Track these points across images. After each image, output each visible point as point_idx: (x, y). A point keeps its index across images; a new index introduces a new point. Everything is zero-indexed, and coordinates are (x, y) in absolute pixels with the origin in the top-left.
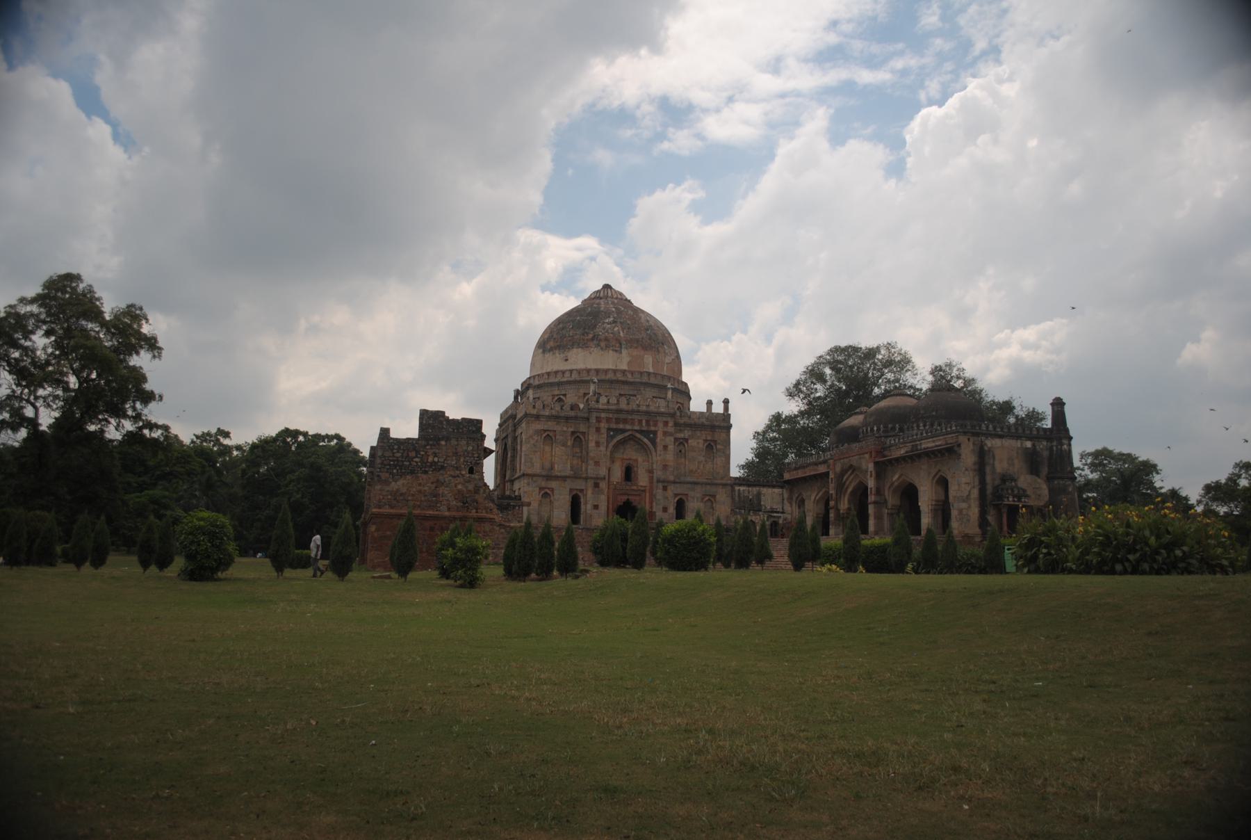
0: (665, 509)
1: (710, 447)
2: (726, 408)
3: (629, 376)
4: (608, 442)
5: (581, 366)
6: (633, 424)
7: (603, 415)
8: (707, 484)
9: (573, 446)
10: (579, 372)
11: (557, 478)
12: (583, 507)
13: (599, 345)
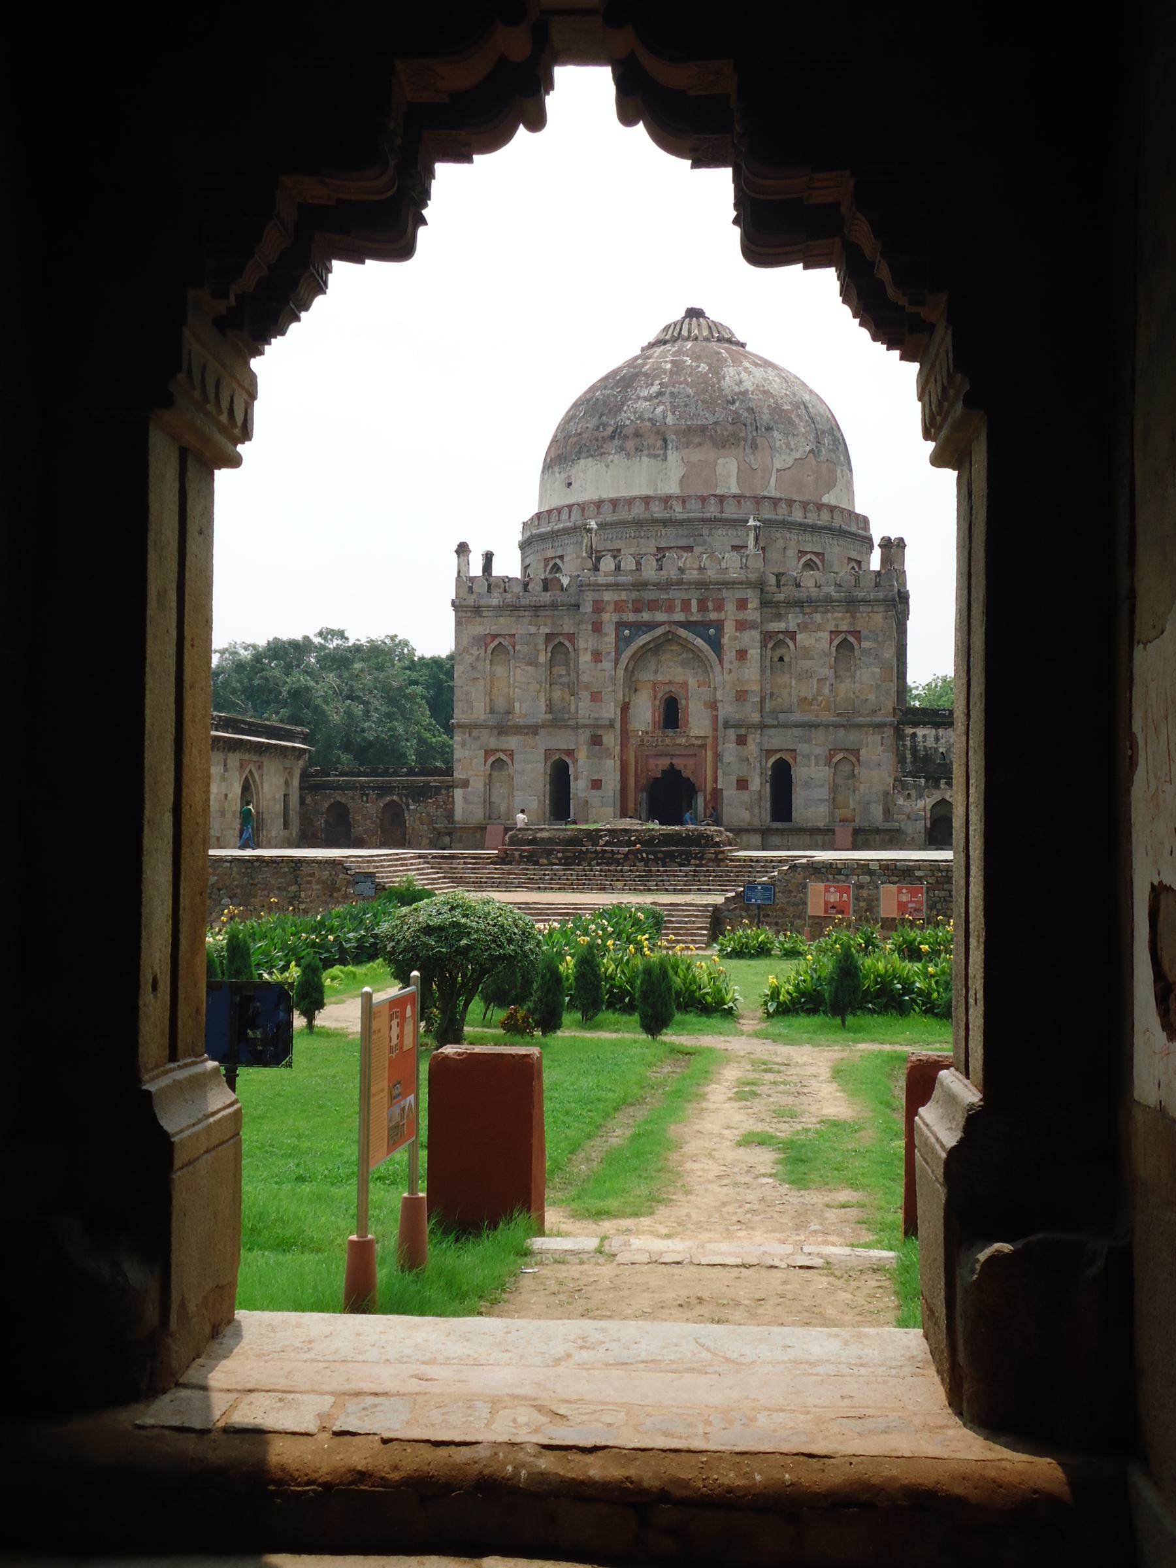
0: (742, 784)
1: (845, 647)
3: (678, 508)
4: (618, 653)
6: (670, 609)
7: (607, 596)
8: (836, 726)
9: (552, 663)
11: (519, 730)
13: (622, 448)
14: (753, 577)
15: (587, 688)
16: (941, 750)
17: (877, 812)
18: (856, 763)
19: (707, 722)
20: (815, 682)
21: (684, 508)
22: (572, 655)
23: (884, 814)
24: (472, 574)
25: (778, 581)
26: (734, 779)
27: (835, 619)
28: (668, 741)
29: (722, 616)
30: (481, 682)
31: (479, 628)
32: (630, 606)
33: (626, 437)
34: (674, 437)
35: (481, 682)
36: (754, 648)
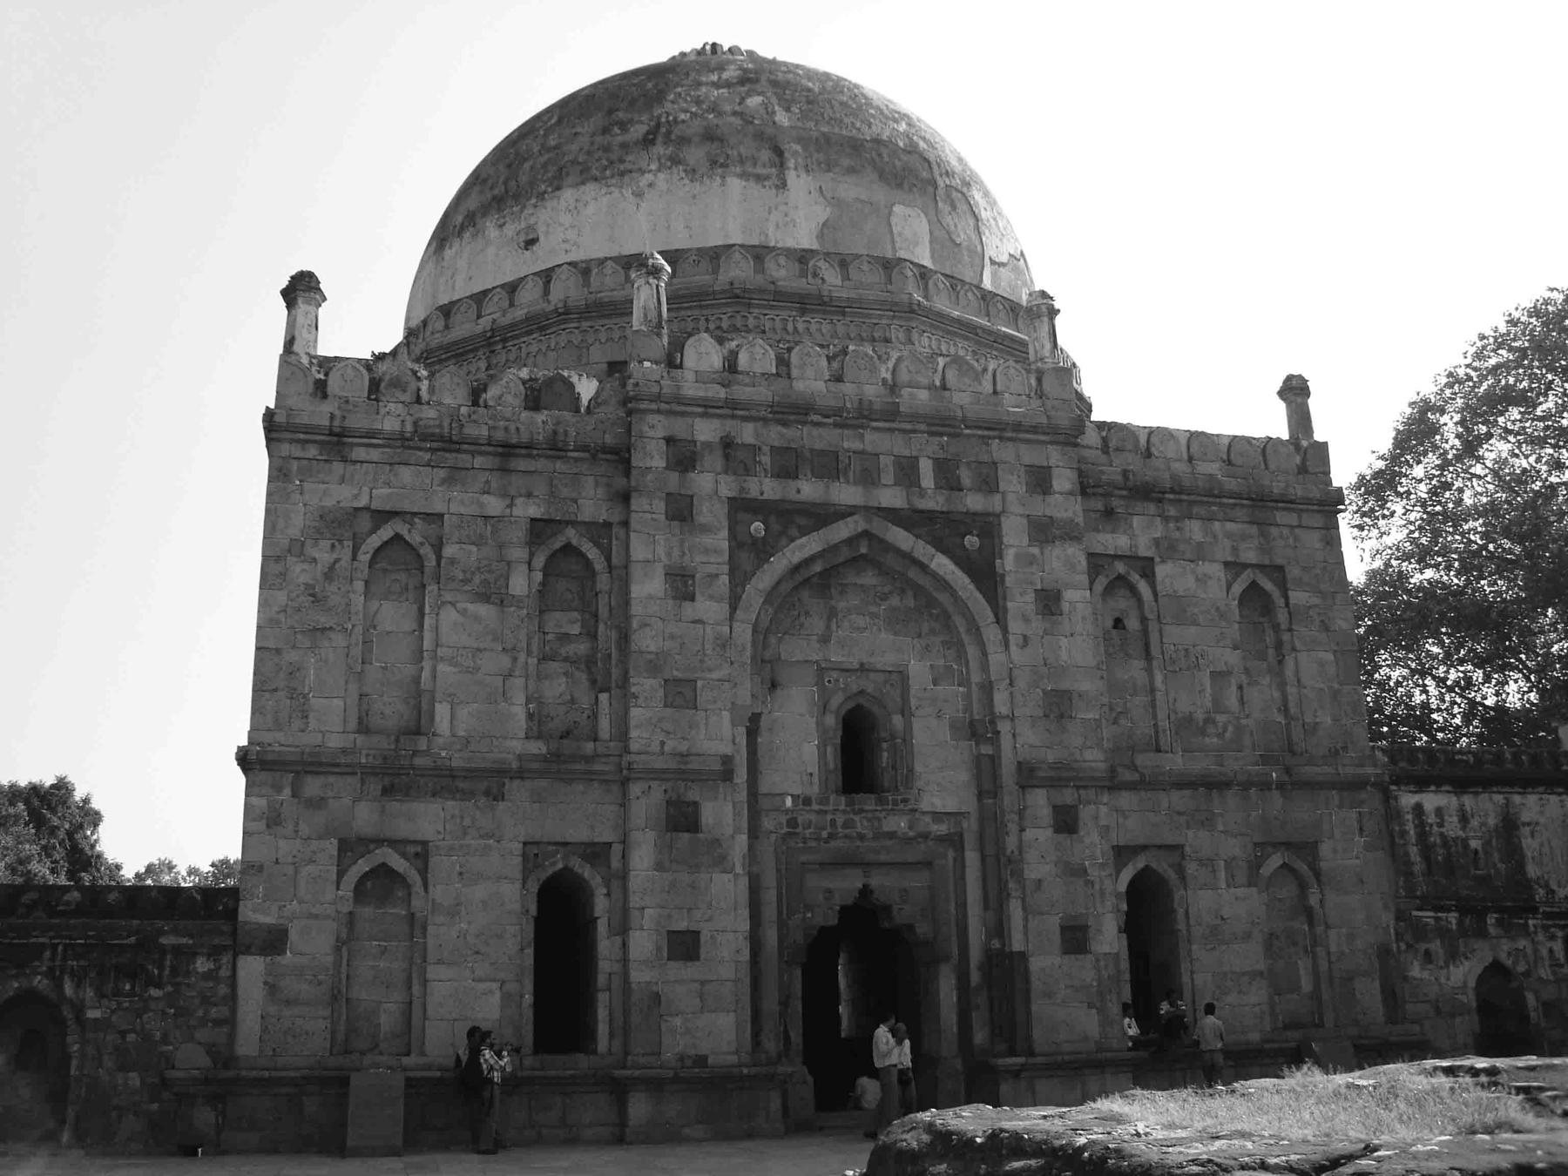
0: (1075, 938)
2: (1300, 419)
3: (832, 277)
4: (739, 578)
5: (593, 247)
6: (869, 478)
7: (706, 431)
9: (544, 599)
10: (584, 270)
11: (448, 782)
12: (605, 946)
13: (675, 161)
14: (1063, 419)
15: (654, 668)
16: (1474, 844)
17: (1369, 993)
18: (1313, 880)
19: (963, 776)
20: (1207, 682)
21: (846, 277)
22: (603, 582)
23: (1385, 1000)
24: (326, 348)
25: (1105, 440)
26: (1053, 923)
27: (1229, 535)
28: (862, 825)
29: (995, 503)
30: (339, 640)
31: (342, 490)
32: (766, 459)
33: (684, 141)
34: (798, 148)
35: (339, 640)
36: (1075, 587)
